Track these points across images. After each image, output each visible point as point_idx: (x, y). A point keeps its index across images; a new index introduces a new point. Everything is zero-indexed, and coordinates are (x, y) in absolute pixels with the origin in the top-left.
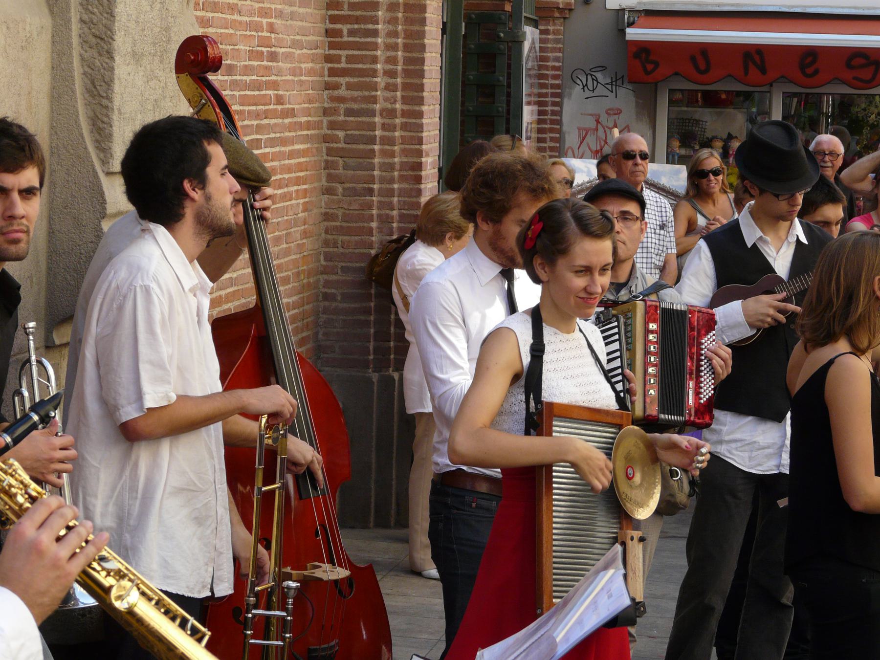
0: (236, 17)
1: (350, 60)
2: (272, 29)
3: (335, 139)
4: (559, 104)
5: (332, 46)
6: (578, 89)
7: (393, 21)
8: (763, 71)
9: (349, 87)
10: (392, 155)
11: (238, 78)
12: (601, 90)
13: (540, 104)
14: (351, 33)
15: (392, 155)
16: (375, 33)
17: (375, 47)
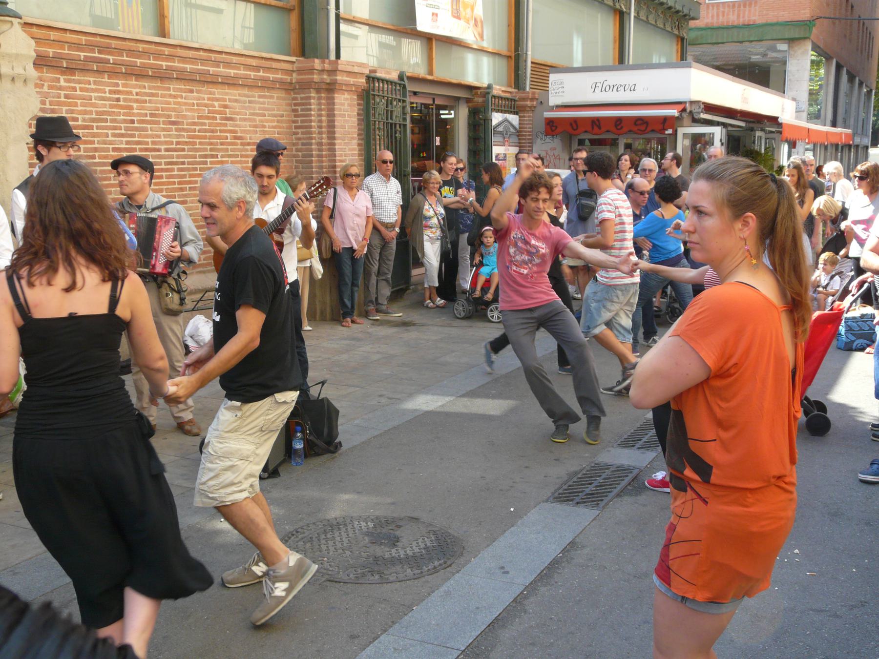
0: (179, 100)
1: (302, 121)
2: (226, 107)
3: (297, 156)
4: (532, 147)
5: (295, 116)
6: (539, 140)
7: (320, 104)
8: (600, 128)
9: (302, 133)
10: (322, 162)
11: (185, 127)
12: (548, 140)
13: (520, 147)
14: (302, 110)
15: (322, 162)
16: (310, 110)
17: (311, 115)
